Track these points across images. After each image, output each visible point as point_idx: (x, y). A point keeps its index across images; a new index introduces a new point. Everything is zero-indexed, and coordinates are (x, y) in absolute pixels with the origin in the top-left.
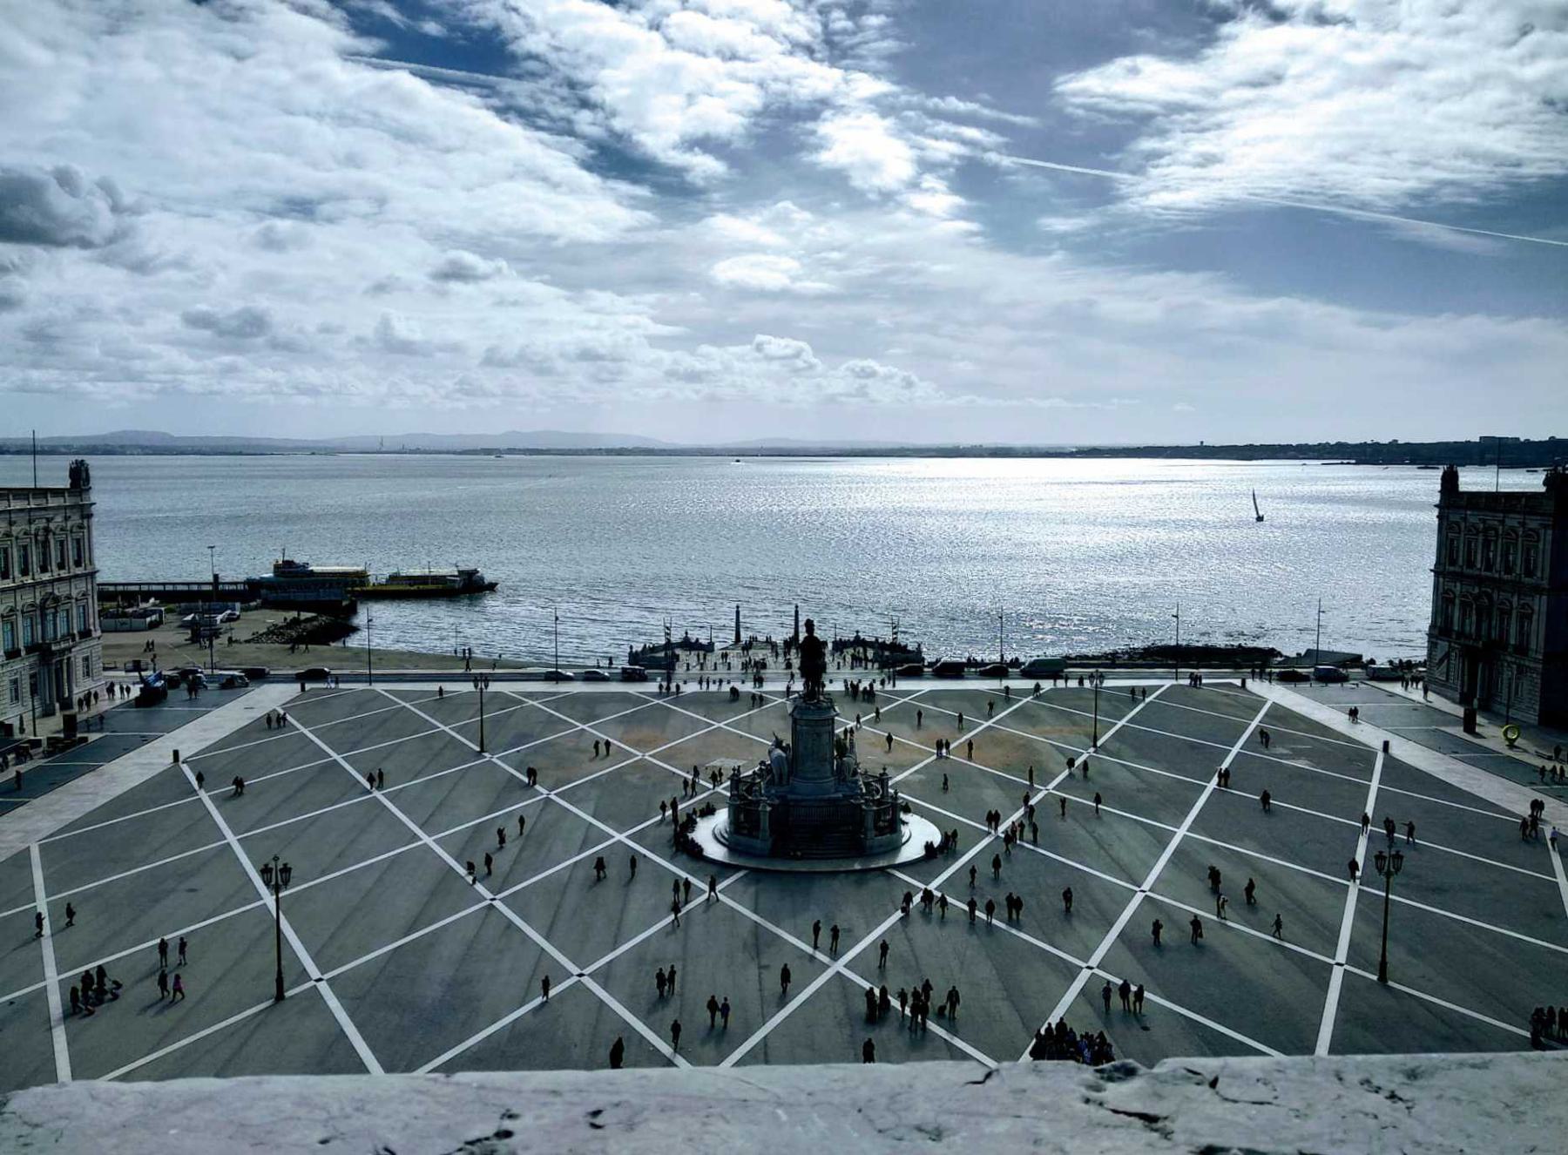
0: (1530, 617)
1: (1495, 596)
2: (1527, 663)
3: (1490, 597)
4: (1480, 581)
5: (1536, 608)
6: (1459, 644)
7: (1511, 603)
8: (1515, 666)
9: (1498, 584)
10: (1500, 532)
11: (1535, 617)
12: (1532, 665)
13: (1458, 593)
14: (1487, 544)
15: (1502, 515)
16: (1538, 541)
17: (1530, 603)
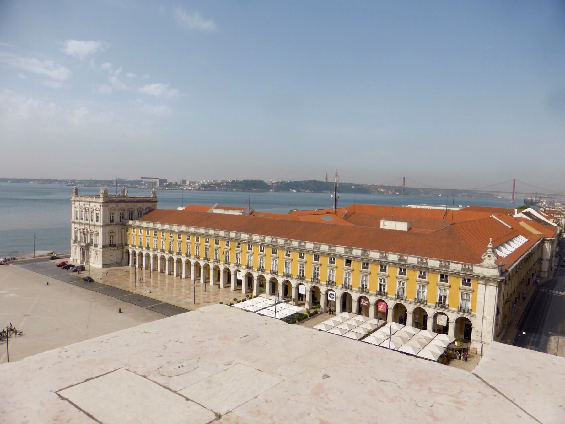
0: (98, 235)
1: (88, 229)
2: (98, 249)
3: (87, 230)
4: (85, 224)
5: (99, 232)
6: (78, 245)
7: (93, 231)
8: (95, 250)
9: (90, 225)
10: (89, 208)
11: (99, 234)
12: (99, 249)
13: (78, 228)
14: (86, 211)
15: (89, 203)
16: (99, 211)
17: (98, 230)
